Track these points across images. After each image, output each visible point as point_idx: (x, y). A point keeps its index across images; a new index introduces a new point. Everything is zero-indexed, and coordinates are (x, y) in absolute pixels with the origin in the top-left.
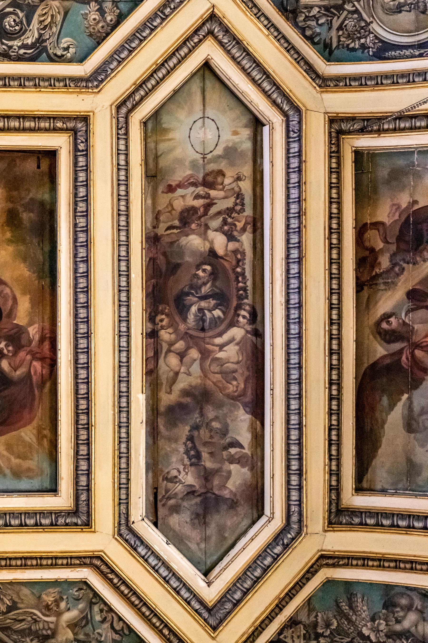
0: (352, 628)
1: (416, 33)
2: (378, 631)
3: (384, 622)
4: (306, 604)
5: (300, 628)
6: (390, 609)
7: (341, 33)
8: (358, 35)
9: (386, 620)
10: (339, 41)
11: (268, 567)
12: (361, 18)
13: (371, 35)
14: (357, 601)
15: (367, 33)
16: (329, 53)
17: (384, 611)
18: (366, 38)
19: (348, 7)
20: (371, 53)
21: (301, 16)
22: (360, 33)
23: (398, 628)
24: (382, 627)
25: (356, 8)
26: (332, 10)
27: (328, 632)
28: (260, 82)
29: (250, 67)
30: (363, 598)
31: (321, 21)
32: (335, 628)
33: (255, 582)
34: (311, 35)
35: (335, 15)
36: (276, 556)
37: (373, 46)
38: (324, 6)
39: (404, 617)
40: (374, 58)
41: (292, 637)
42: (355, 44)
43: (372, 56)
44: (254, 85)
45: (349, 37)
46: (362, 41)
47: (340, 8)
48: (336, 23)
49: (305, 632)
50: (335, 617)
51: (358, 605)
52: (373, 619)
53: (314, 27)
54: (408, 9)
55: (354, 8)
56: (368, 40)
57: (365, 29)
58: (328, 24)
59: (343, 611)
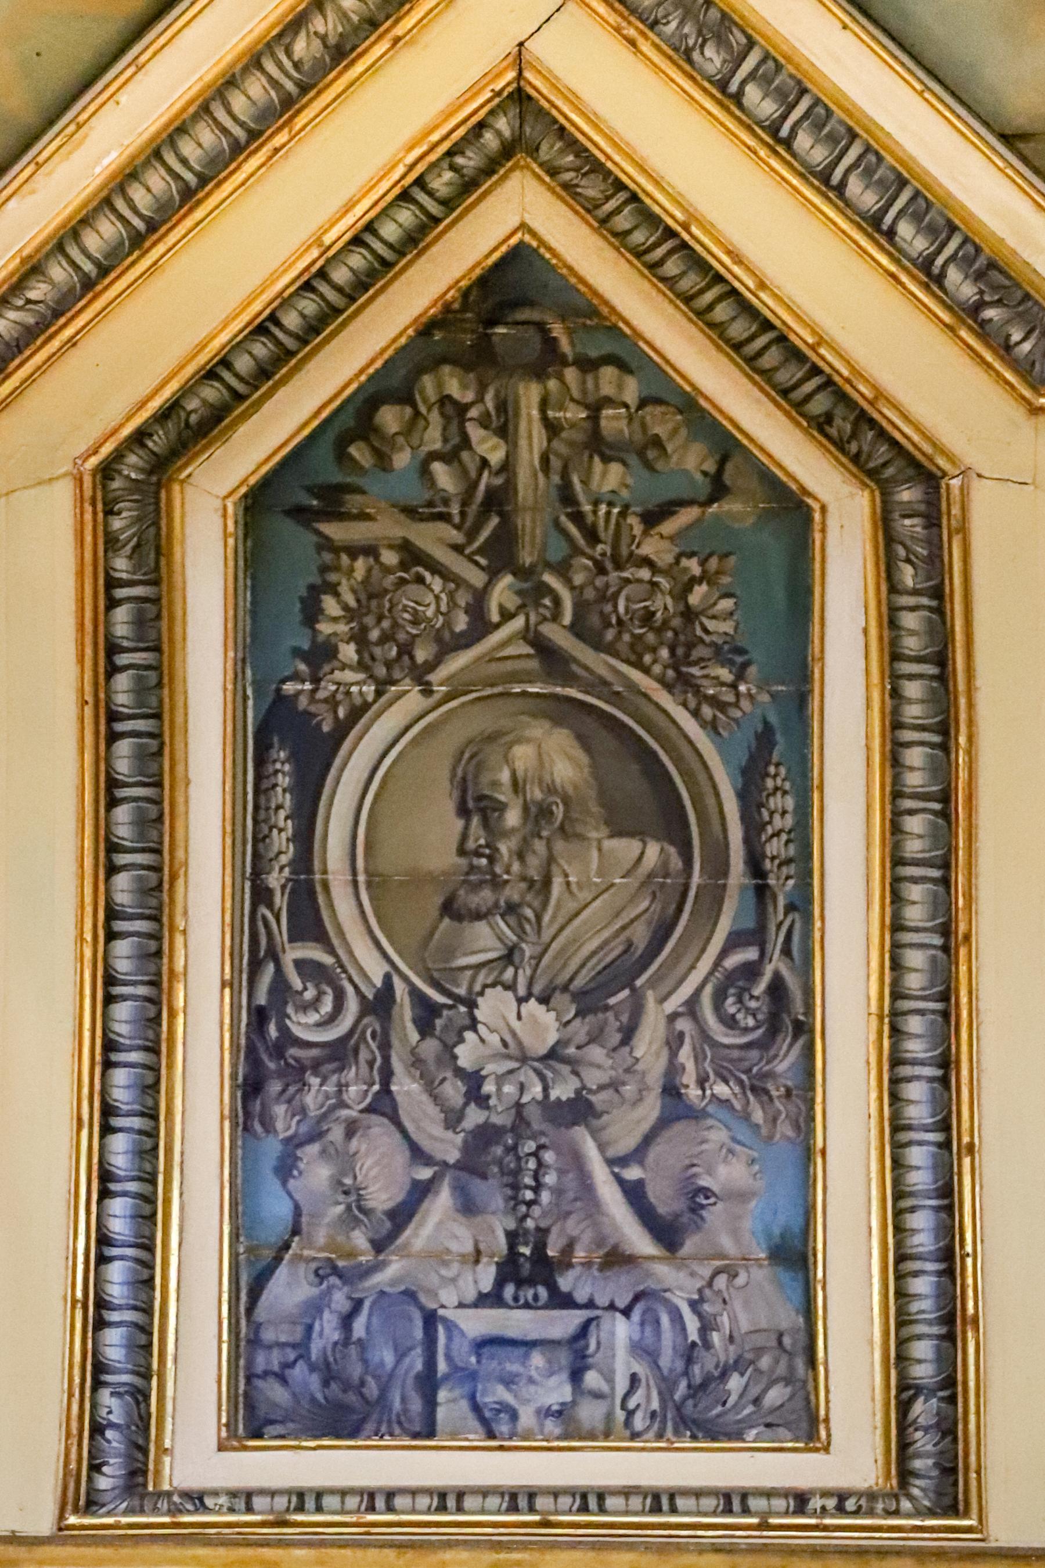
1: (361, 878)
7: (390, 558)
8: (374, 635)
10: (354, 551)
12: (449, 645)
13: (369, 689)
15: (381, 671)
16: (281, 506)
18: (361, 666)
19: (503, 592)
20: (289, 687)
21: (464, 387)
22: (386, 638)
25: (497, 626)
26: (495, 521)
28: (120, 204)
29: (184, 162)
31: (443, 475)
34: (376, 430)
35: (471, 535)
37: (321, 695)
38: (510, 485)
40: (269, 699)
42: (335, 620)
43: (278, 690)
44: (113, 177)
45: (371, 593)
46: (349, 652)
47: (501, 555)
48: (433, 539)
53: (415, 442)
54: (471, 845)
55: (495, 618)
56: (349, 676)
57: (398, 662)
58: (430, 504)
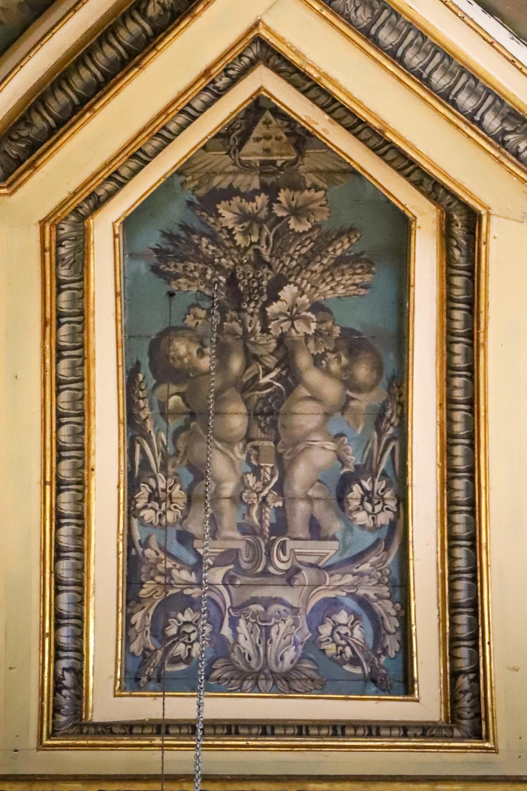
0: (294, 263)
2: (292, 319)
3: (311, 332)
4: (345, 167)
5: (289, 154)
6: (342, 343)
9: (318, 332)
11: (454, 103)
14: (355, 274)
17: (337, 331)
23: (303, 360)
24: (300, 327)
27: (280, 214)
30: (362, 287)
32: (291, 227)
33: (419, 75)
36: (477, 118)
39: (327, 372)
41: (268, 138)
49: (279, 164)
50: (316, 226)
51: (347, 277)
52: (317, 307)
59: (330, 244)
